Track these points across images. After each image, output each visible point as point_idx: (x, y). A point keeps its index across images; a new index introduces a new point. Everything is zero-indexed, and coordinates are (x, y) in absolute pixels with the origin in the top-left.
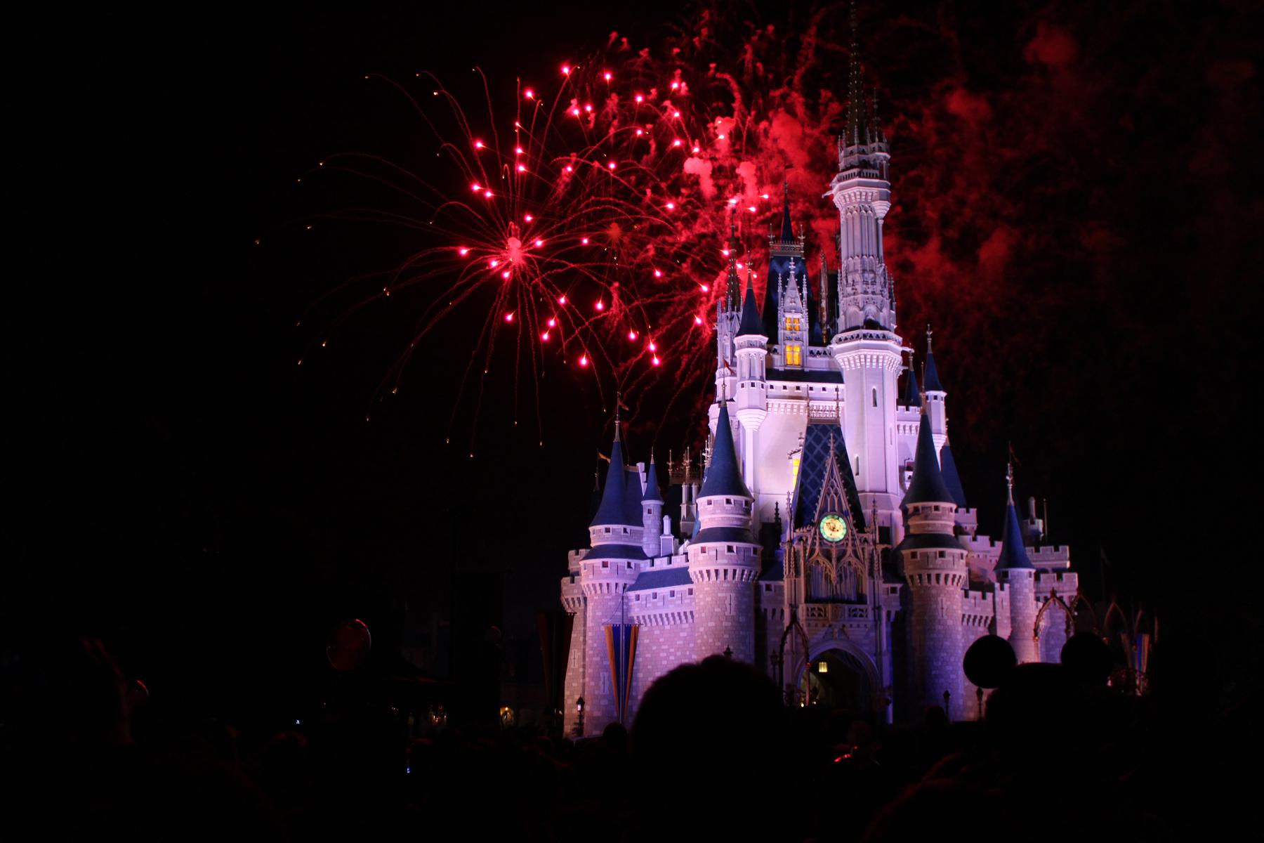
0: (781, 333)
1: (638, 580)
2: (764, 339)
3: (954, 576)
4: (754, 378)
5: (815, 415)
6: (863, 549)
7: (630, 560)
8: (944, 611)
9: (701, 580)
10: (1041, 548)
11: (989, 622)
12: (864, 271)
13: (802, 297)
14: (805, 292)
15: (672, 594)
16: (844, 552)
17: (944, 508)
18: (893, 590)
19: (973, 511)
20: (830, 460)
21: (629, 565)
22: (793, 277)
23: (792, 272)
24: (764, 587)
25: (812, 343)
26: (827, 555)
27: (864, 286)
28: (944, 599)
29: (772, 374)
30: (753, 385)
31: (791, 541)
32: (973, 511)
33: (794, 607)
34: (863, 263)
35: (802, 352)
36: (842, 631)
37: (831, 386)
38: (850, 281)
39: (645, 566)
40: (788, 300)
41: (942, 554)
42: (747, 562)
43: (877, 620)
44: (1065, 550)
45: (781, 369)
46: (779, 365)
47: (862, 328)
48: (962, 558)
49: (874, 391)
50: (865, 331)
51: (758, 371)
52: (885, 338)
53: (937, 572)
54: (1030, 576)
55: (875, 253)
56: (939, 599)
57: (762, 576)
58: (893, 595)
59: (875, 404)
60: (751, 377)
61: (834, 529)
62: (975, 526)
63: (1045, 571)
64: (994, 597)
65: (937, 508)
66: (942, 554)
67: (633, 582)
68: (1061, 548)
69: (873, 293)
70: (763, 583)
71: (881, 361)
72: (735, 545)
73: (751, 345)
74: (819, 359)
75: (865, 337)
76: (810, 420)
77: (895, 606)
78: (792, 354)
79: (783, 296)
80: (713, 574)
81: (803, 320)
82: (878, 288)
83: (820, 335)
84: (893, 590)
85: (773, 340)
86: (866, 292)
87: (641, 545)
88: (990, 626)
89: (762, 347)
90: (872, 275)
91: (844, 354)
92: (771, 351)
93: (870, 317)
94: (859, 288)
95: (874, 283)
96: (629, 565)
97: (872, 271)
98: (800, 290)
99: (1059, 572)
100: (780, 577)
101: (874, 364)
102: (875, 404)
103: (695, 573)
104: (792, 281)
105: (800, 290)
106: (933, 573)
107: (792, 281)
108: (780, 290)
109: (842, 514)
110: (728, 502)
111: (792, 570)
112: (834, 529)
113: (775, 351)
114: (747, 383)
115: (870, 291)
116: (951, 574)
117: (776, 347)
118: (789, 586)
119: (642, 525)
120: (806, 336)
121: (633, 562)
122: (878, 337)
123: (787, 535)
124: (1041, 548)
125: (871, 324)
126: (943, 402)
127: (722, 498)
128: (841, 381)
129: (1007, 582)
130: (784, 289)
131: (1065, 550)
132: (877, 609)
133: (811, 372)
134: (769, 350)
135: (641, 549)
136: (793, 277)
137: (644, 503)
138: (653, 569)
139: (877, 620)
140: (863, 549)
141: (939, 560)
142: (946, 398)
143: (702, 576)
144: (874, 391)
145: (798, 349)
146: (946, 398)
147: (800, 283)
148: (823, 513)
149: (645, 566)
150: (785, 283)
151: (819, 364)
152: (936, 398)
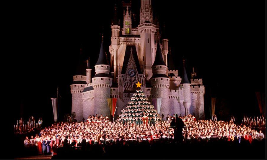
0: (124, 25)
1: (84, 90)
2: (119, 27)
3: (167, 85)
4: (116, 37)
6: (140, 78)
7: (82, 85)
8: (163, 94)
9: (96, 87)
10: (195, 80)
11: (177, 98)
12: (146, 8)
13: (130, 16)
14: (131, 15)
17: (163, 67)
18: (149, 90)
19: (177, 71)
21: (82, 86)
22: (127, 11)
23: (127, 10)
24: (113, 90)
27: (146, 12)
28: (163, 92)
30: (116, 38)
32: (177, 71)
34: (145, 6)
38: (142, 11)
40: (126, 17)
44: (201, 80)
45: (124, 34)
47: (145, 23)
48: (168, 80)
49: (148, 39)
50: (145, 24)
52: (151, 25)
53: (160, 84)
54: (189, 86)
55: (149, 4)
56: (161, 91)
58: (149, 91)
59: (148, 43)
60: (115, 36)
62: (178, 74)
63: (196, 85)
64: (179, 91)
65: (161, 67)
66: (162, 79)
67: (83, 90)
68: (200, 79)
69: (148, 14)
70: (113, 88)
71: (150, 31)
73: (115, 28)
74: (134, 31)
75: (145, 25)
76: (127, 45)
79: (125, 16)
80: (99, 86)
81: (130, 22)
82: (149, 13)
84: (149, 90)
86: (146, 14)
87: (85, 81)
88: (178, 99)
89: (119, 29)
90: (148, 10)
91: (140, 29)
92: (121, 29)
93: (147, 20)
94: (145, 13)
95: (148, 12)
96: (82, 86)
97: (148, 9)
99: (199, 85)
101: (148, 32)
102: (148, 43)
103: (94, 86)
104: (127, 12)
105: (130, 15)
106: (159, 84)
107: (127, 12)
108: (124, 15)
110: (102, 66)
111: (120, 85)
113: (123, 30)
114: (114, 38)
115: (147, 13)
116: (164, 84)
117: (123, 29)
119: (86, 75)
121: (83, 85)
122: (149, 25)
124: (195, 80)
125: (147, 22)
126: (167, 42)
127: (100, 65)
129: (182, 87)
130: (125, 14)
131: (201, 80)
133: (132, 35)
135: (86, 81)
136: (127, 11)
138: (87, 87)
140: (140, 78)
141: (161, 81)
142: (169, 42)
143: (96, 86)
144: (148, 39)
146: (168, 41)
149: (86, 86)
150: (126, 13)
151: (135, 33)
152: (165, 41)
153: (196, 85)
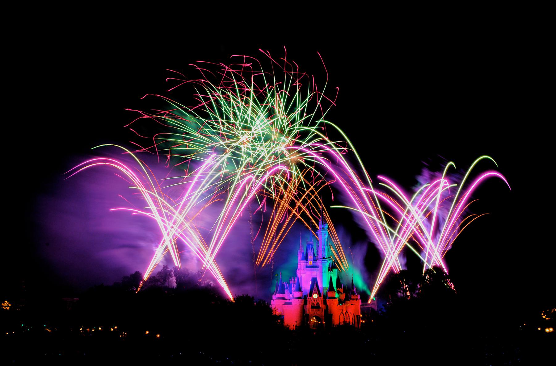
0: (308, 260)
2: (305, 261)
5: (313, 277)
14: (313, 252)
15: (290, 306)
16: (317, 300)
20: (315, 285)
25: (314, 261)
26: (315, 301)
29: (307, 267)
31: (308, 299)
33: (309, 309)
35: (312, 263)
36: (316, 313)
37: (317, 269)
39: (286, 301)
41: (333, 300)
42: (301, 302)
43: (322, 311)
46: (308, 265)
47: (322, 259)
51: (305, 267)
52: (326, 261)
57: (304, 304)
61: (315, 296)
63: (354, 299)
66: (333, 300)
72: (299, 300)
73: (303, 262)
77: (325, 309)
78: (311, 263)
83: (315, 260)
84: (325, 306)
85: (307, 260)
89: (305, 262)
98: (312, 251)
99: (357, 299)
100: (307, 304)
105: (312, 251)
107: (310, 249)
108: (308, 251)
109: (317, 293)
112: (315, 296)
118: (309, 306)
120: (313, 259)
121: (284, 300)
123: (308, 298)
128: (318, 268)
132: (322, 309)
134: (306, 262)
135: (285, 298)
137: (285, 290)
139: (322, 311)
145: (311, 262)
147: (312, 250)
148: (314, 294)
150: (309, 250)
151: (315, 264)
153: (354, 299)
